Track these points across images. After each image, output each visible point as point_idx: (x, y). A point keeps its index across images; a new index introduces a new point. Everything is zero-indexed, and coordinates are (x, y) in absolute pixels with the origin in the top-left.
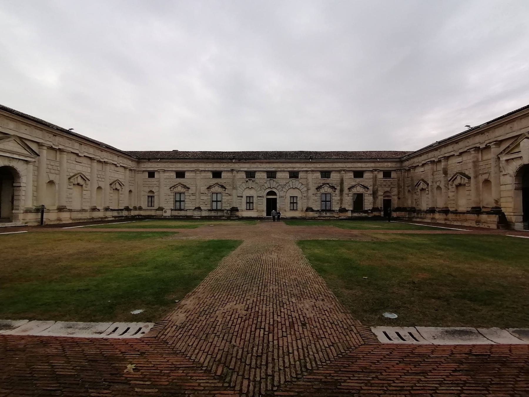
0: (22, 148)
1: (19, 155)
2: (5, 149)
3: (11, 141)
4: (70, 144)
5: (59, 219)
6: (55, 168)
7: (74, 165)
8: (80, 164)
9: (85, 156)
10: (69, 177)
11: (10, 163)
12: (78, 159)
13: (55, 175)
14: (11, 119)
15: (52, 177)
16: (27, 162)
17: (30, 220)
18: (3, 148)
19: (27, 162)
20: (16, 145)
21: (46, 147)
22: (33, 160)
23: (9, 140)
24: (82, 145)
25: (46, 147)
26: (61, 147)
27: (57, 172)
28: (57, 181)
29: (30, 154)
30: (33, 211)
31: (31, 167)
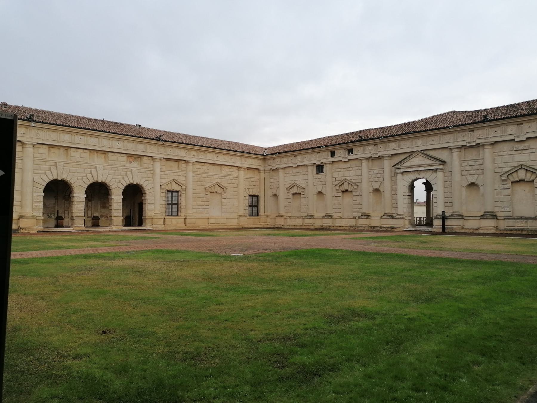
0: (427, 159)
1: (424, 167)
2: (411, 165)
3: (416, 157)
4: (499, 132)
5: (497, 228)
6: (476, 167)
7: (512, 156)
8: (524, 152)
9: (528, 139)
10: (502, 173)
11: (419, 175)
12: (518, 146)
13: (476, 176)
14: (418, 137)
15: (472, 179)
16: (436, 170)
17: (437, 226)
18: (410, 165)
19: (436, 170)
20: (421, 158)
21: (455, 148)
22: (441, 167)
23: (412, 156)
24: (524, 124)
25: (455, 148)
26: (478, 142)
27: (480, 171)
28: (479, 183)
29: (435, 162)
30: (439, 218)
31: (440, 174)
